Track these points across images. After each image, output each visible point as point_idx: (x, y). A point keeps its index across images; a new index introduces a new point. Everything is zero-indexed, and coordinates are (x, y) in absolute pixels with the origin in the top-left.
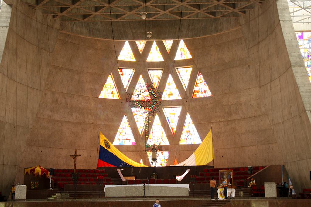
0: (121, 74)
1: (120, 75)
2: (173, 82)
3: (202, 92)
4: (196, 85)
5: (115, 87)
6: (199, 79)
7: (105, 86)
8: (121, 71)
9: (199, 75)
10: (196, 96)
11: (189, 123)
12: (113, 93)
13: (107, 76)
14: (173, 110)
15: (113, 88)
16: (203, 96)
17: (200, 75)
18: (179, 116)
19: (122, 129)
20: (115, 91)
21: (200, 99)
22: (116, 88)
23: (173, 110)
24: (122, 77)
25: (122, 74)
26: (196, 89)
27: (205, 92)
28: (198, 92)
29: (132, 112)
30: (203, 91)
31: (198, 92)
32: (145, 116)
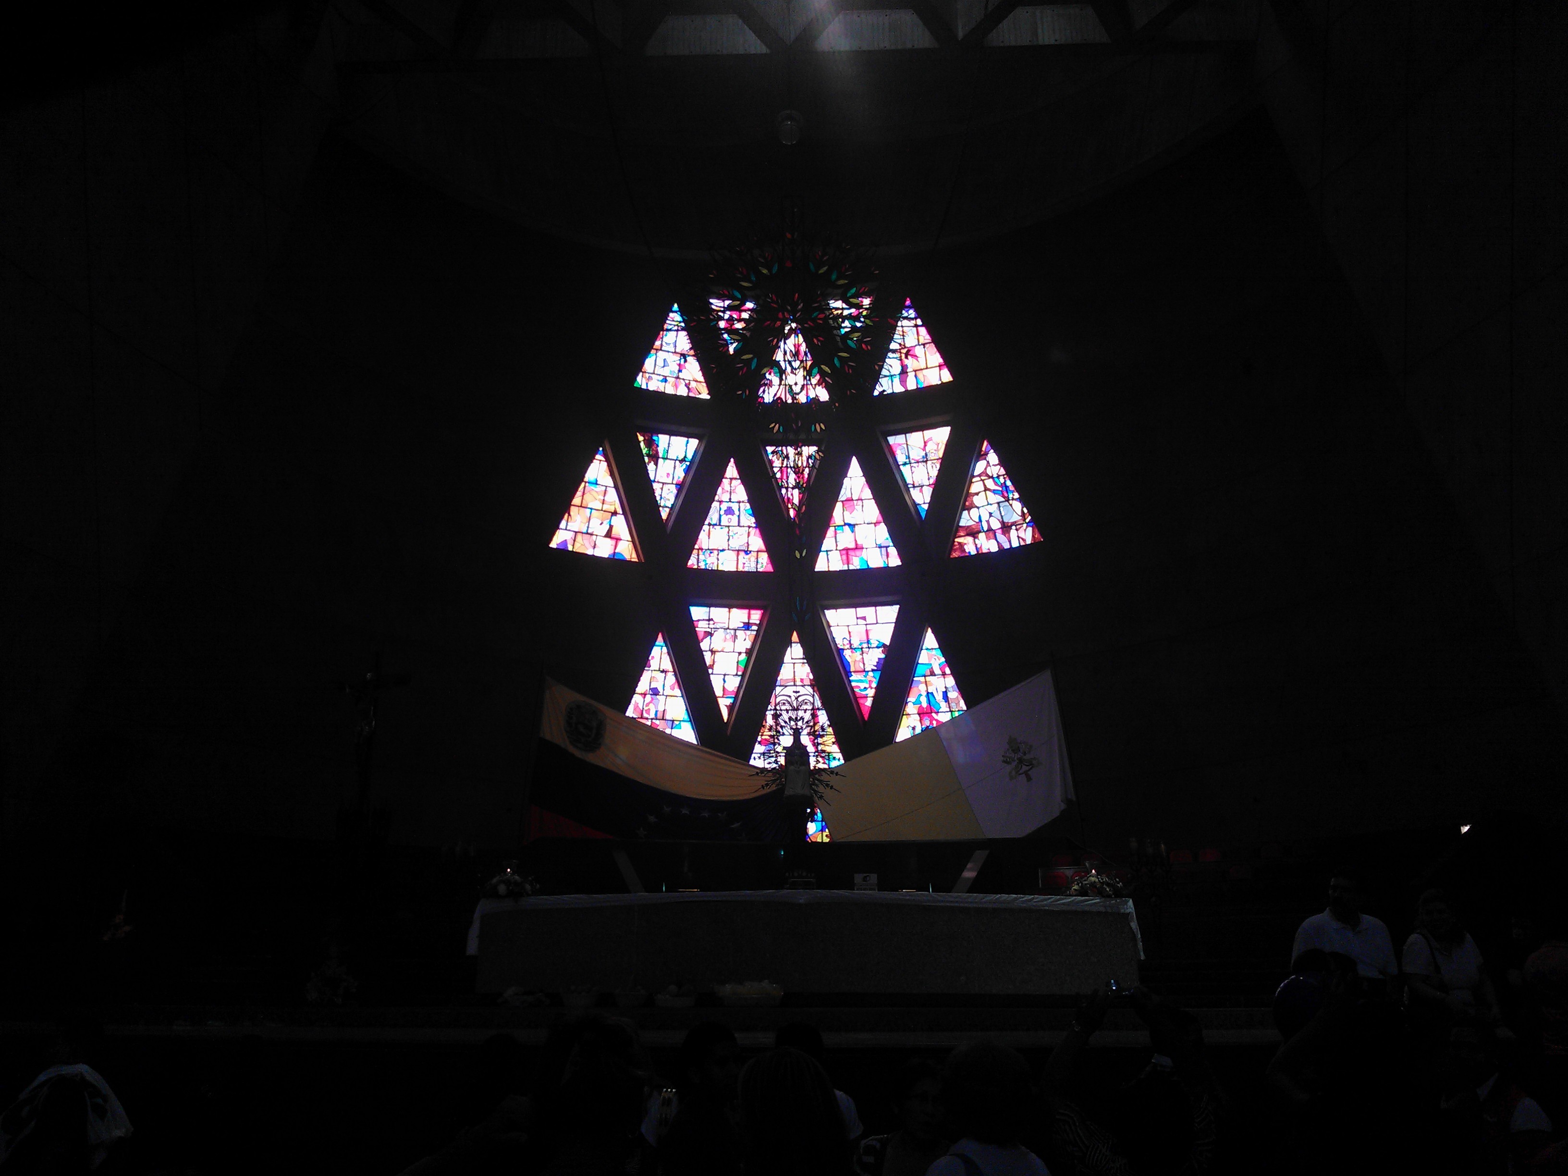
0: (648, 455)
1: (646, 459)
2: (868, 493)
3: (990, 529)
4: (965, 500)
5: (620, 511)
6: (980, 476)
7: (576, 500)
8: (650, 443)
9: (983, 456)
10: (964, 551)
11: (932, 674)
12: (614, 532)
13: (591, 459)
14: (864, 618)
15: (615, 513)
16: (994, 548)
17: (986, 454)
18: (887, 642)
19: (648, 698)
20: (621, 526)
21: (982, 557)
22: (624, 513)
23: (864, 618)
24: (651, 467)
25: (655, 458)
26: (966, 519)
27: (1006, 528)
28: (973, 533)
29: (691, 624)
30: (996, 525)
31: (973, 533)
32: (745, 641)
